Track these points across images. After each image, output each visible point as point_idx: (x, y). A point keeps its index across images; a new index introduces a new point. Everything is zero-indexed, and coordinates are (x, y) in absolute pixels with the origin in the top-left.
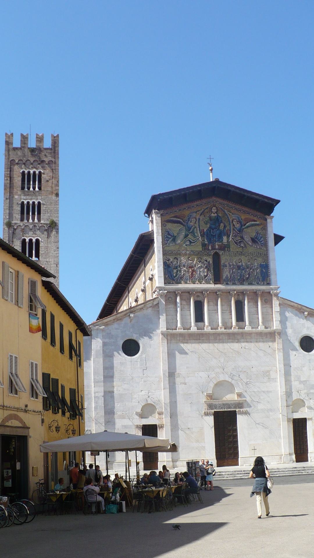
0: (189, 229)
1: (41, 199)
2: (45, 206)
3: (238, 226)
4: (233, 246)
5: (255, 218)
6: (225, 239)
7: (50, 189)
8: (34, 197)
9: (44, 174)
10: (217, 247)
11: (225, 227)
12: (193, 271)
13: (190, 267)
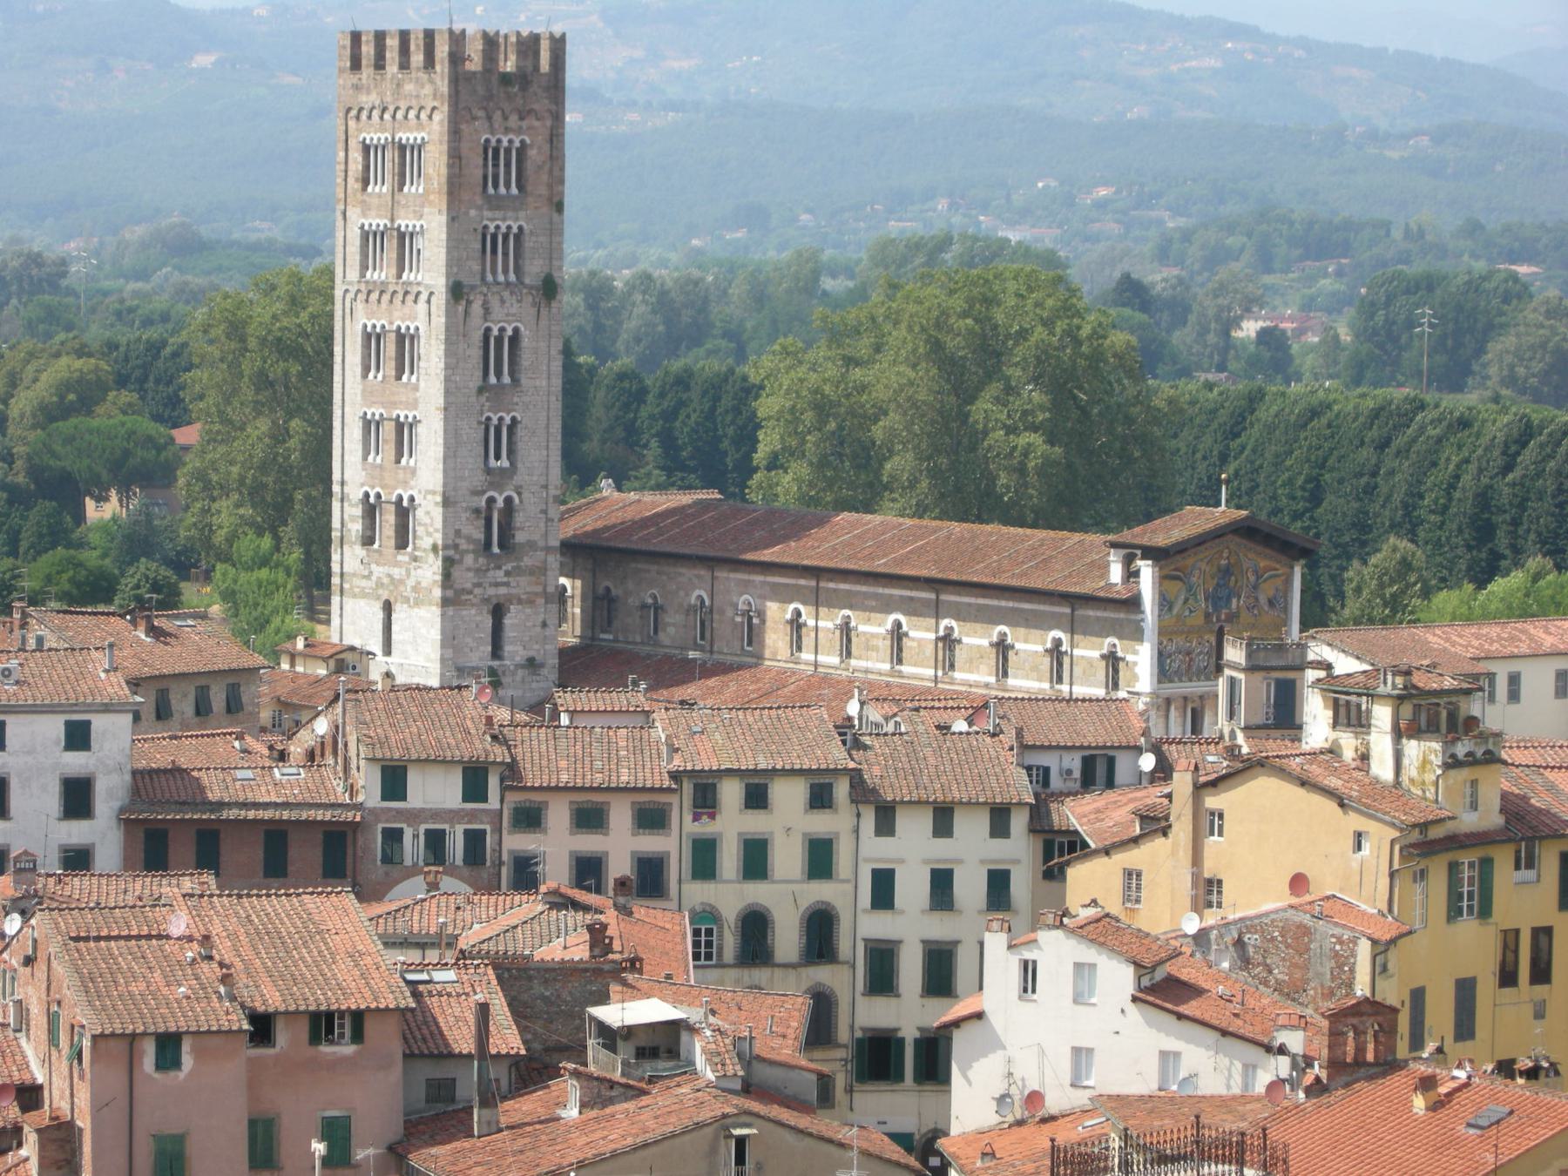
0: (1189, 589)
1: (529, 219)
2: (534, 239)
3: (1252, 578)
4: (1244, 615)
5: (1278, 566)
6: (1234, 601)
7: (544, 191)
8: (510, 214)
9: (532, 146)
10: (1223, 617)
11: (1236, 582)
12: (1191, 660)
13: (1188, 654)
